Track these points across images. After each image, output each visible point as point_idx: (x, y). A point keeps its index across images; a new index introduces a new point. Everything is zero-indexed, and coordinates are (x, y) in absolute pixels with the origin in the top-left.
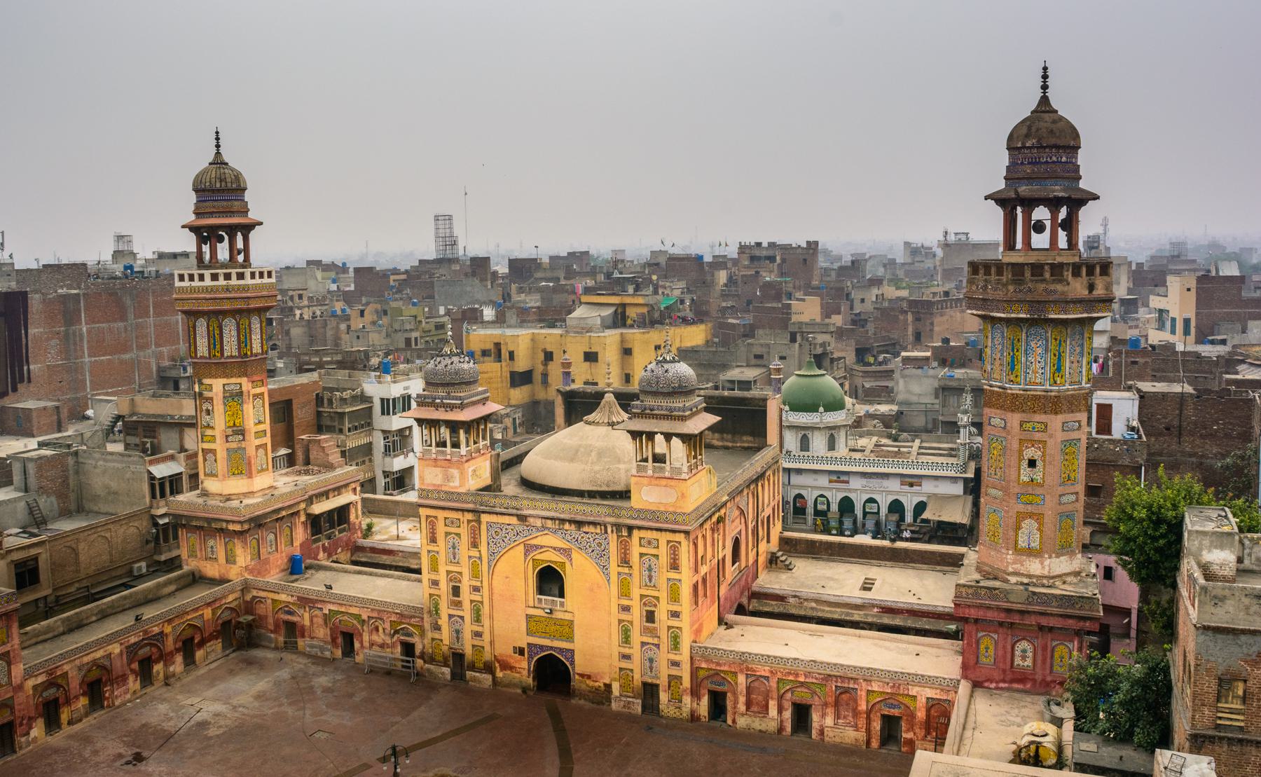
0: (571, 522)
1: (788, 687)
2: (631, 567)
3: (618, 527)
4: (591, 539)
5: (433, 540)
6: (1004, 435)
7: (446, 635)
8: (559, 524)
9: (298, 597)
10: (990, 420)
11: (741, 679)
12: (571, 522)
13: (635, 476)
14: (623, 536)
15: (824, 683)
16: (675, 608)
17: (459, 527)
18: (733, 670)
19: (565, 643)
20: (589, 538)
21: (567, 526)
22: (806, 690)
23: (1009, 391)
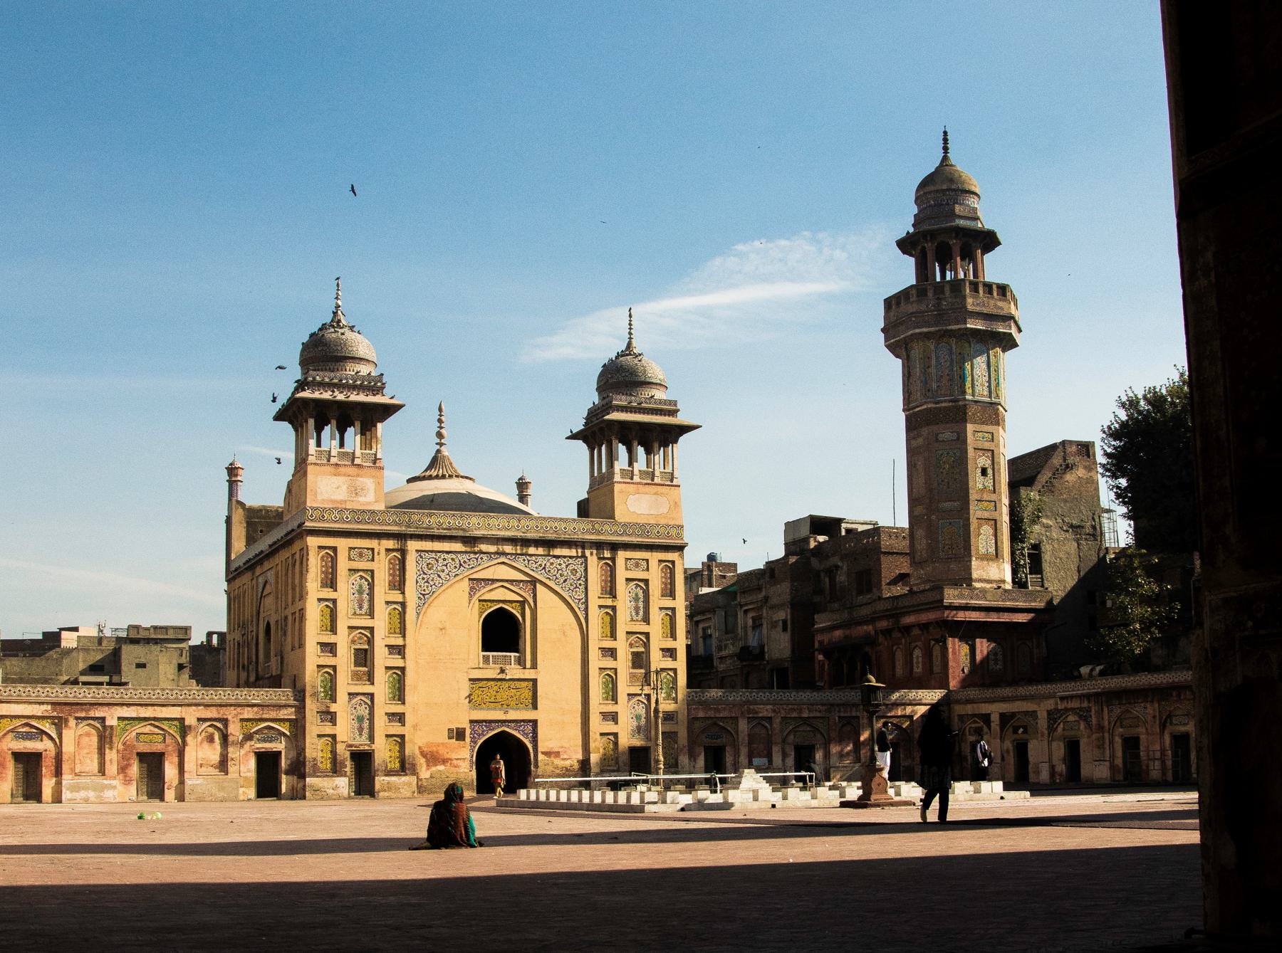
0: (538, 543)
1: (791, 727)
2: (615, 597)
3: (599, 546)
4: (564, 566)
5: (330, 581)
6: (959, 446)
7: (345, 730)
8: (522, 550)
9: (53, 704)
10: (937, 435)
11: (743, 725)
12: (538, 543)
13: (620, 483)
14: (604, 558)
15: (827, 715)
16: (670, 644)
17: (373, 560)
18: (734, 715)
19: (525, 712)
20: (560, 564)
21: (532, 550)
22: (808, 729)
23: (960, 403)
